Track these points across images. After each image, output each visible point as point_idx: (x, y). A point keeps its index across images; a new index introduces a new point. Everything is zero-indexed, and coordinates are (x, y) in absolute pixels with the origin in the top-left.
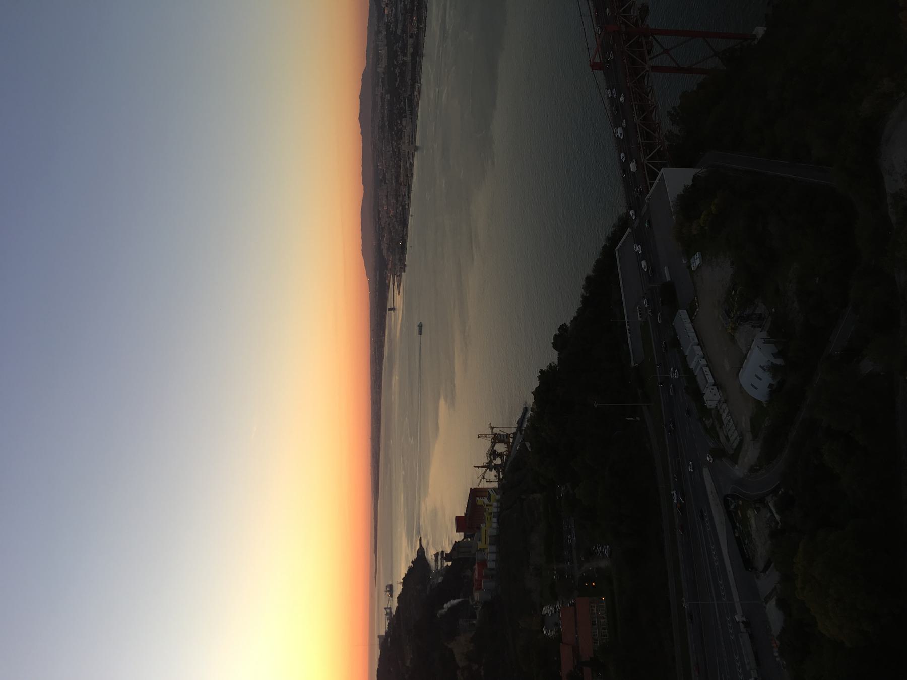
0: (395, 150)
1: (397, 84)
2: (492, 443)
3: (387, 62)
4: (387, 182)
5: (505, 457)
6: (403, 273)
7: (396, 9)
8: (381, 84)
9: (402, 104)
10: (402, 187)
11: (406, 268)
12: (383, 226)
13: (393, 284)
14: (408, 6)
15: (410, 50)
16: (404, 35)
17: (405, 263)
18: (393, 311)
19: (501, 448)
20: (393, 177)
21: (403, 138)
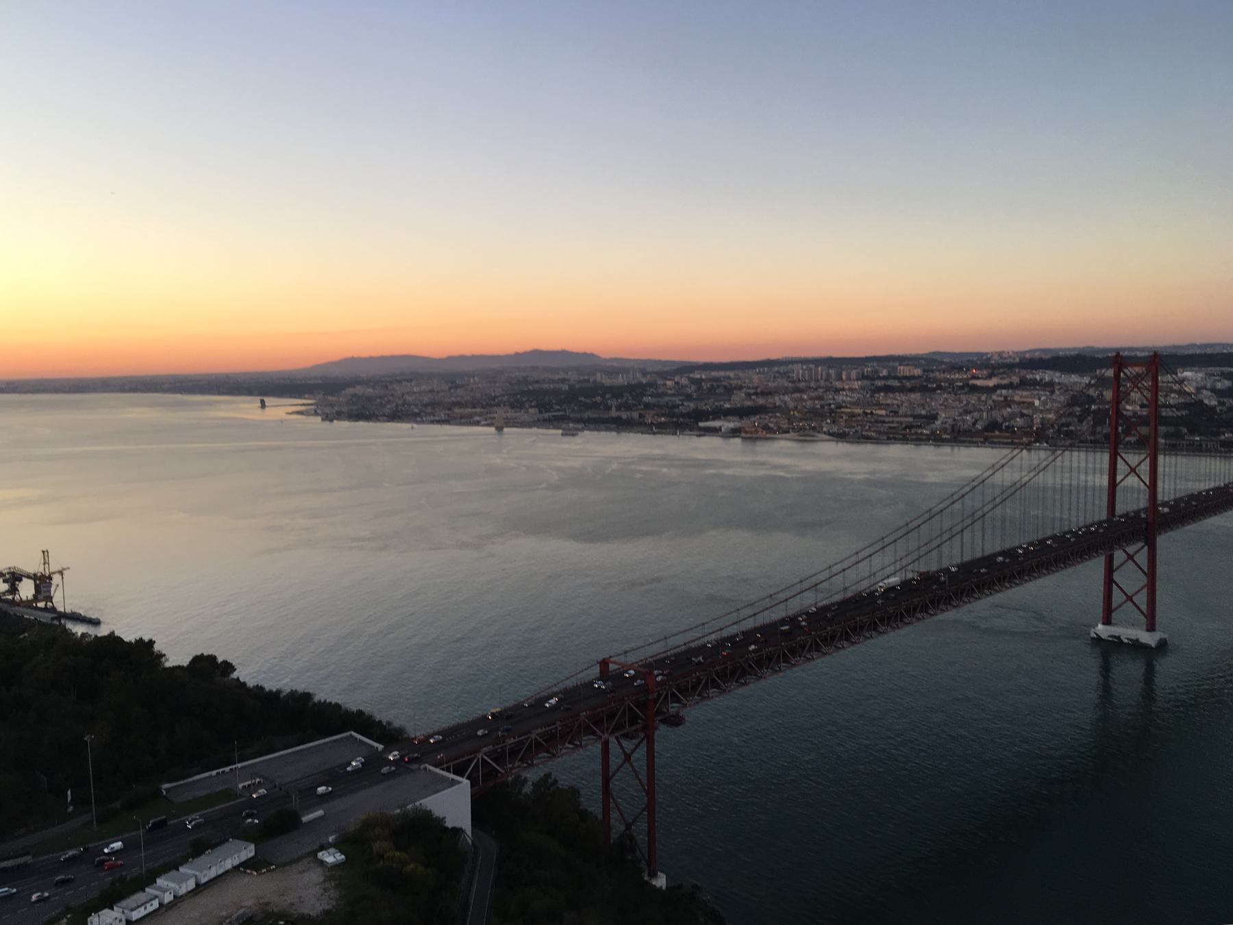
0: (496, 400)
1: (582, 399)
2: (35, 575)
3: (608, 385)
4: (452, 391)
5: (10, 597)
6: (319, 419)
7: (673, 395)
8: (581, 378)
9: (558, 407)
10: (447, 412)
11: (328, 422)
12: (389, 387)
13: (304, 405)
14: (676, 411)
15: (624, 415)
16: (642, 407)
17: (335, 422)
18: (260, 405)
19: (26, 590)
20: (459, 399)
21: (513, 411)
